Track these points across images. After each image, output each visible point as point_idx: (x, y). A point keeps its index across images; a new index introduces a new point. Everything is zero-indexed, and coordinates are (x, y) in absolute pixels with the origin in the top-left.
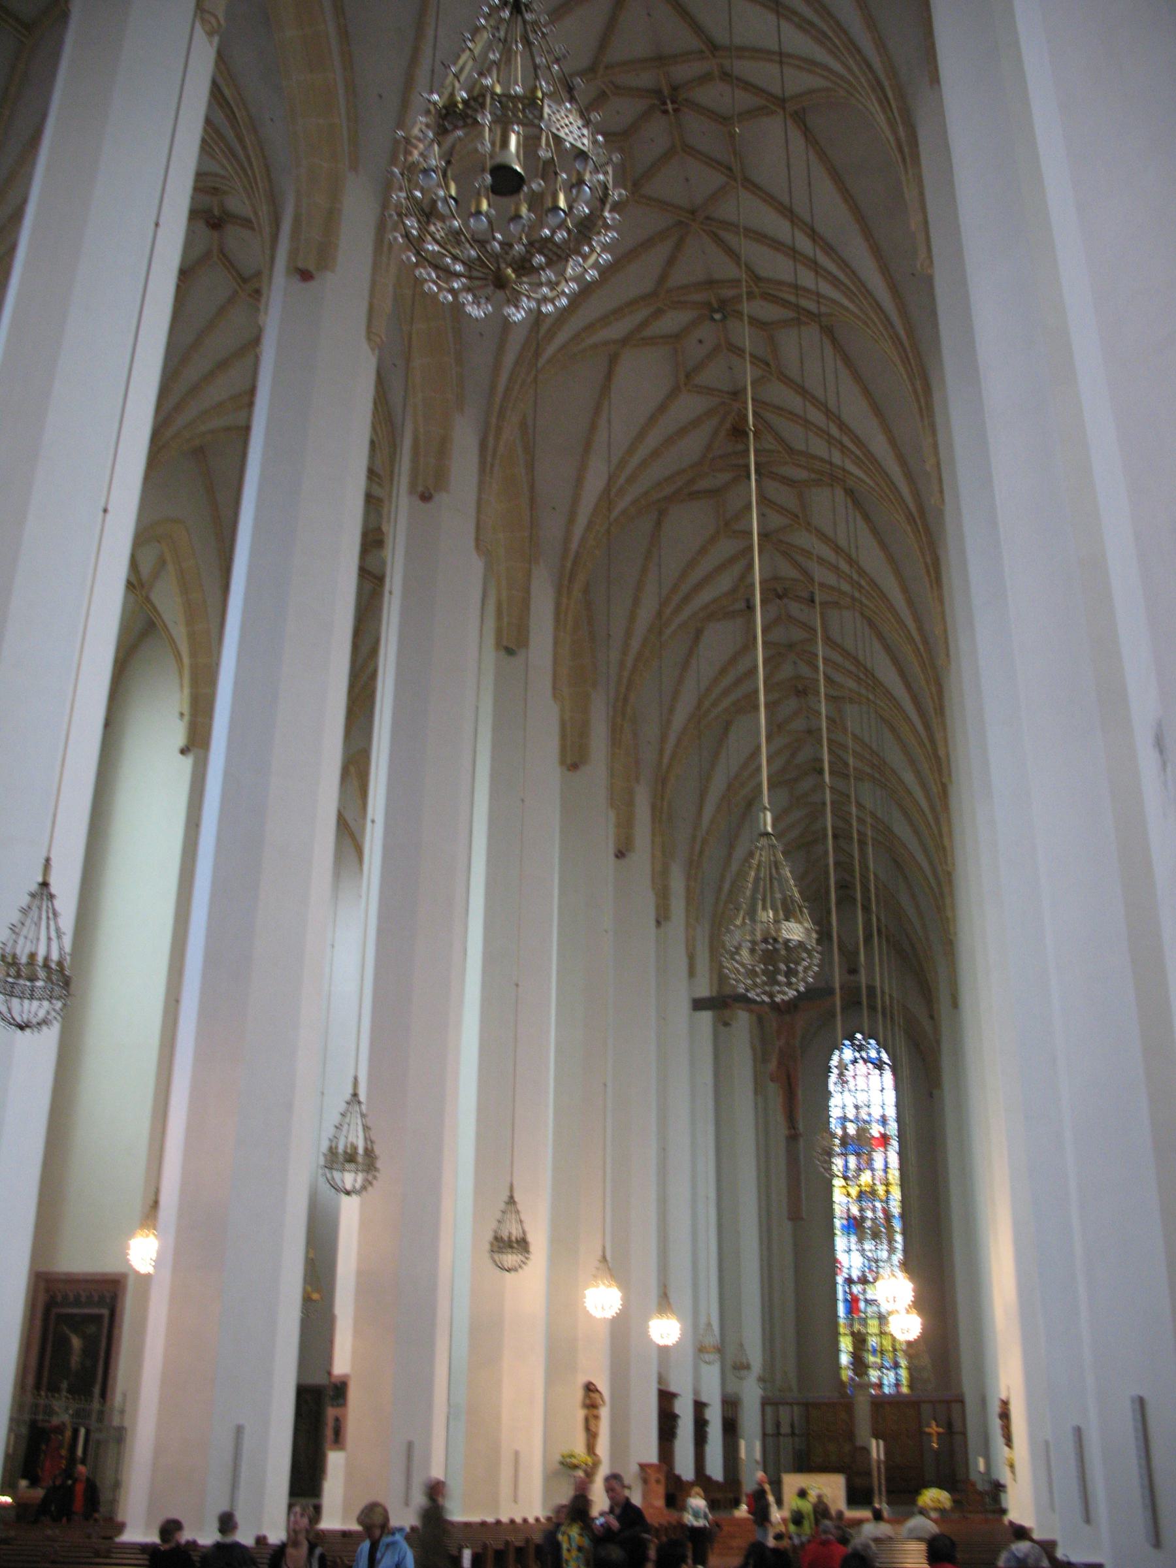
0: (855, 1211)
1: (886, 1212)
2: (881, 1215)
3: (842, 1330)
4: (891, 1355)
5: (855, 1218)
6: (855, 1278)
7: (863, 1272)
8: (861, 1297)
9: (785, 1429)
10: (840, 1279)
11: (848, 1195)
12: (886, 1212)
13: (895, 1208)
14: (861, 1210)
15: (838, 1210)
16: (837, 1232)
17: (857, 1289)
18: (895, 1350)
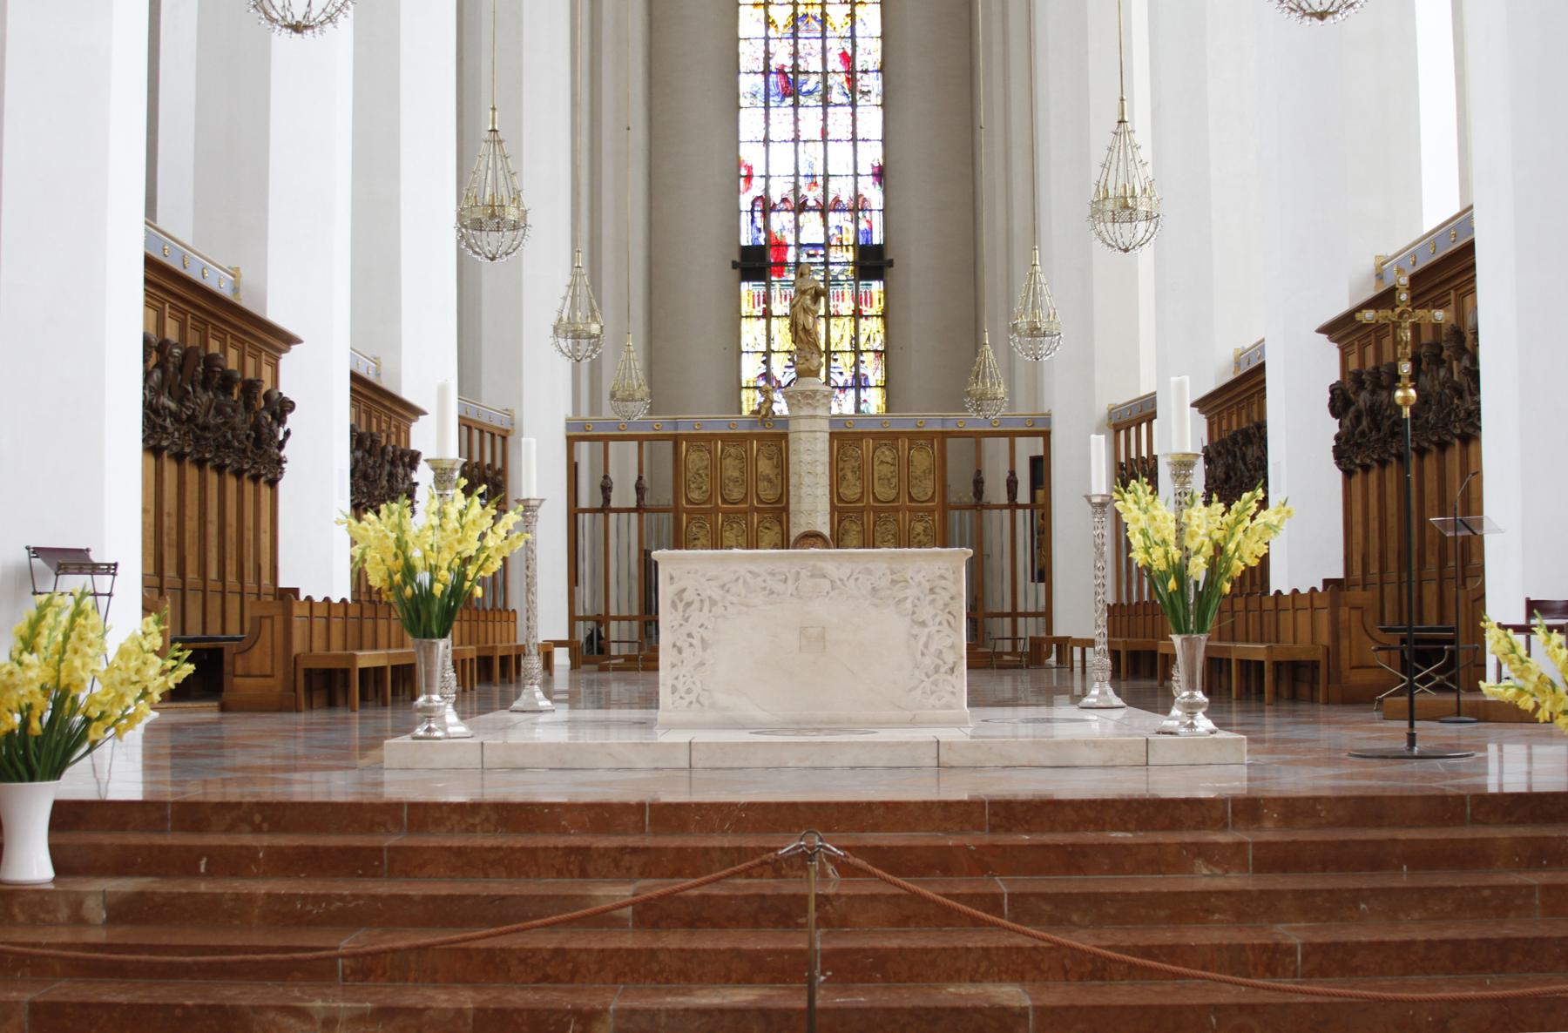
0: (781, 57)
1: (848, 59)
2: (841, 68)
3: (746, 308)
4: (849, 359)
5: (781, 71)
6: (776, 198)
7: (796, 188)
8: (790, 239)
9: (624, 495)
10: (745, 202)
11: (769, 23)
12: (848, 59)
13: (869, 54)
14: (795, 55)
15: (750, 56)
16: (743, 102)
17: (781, 222)
18: (857, 352)
